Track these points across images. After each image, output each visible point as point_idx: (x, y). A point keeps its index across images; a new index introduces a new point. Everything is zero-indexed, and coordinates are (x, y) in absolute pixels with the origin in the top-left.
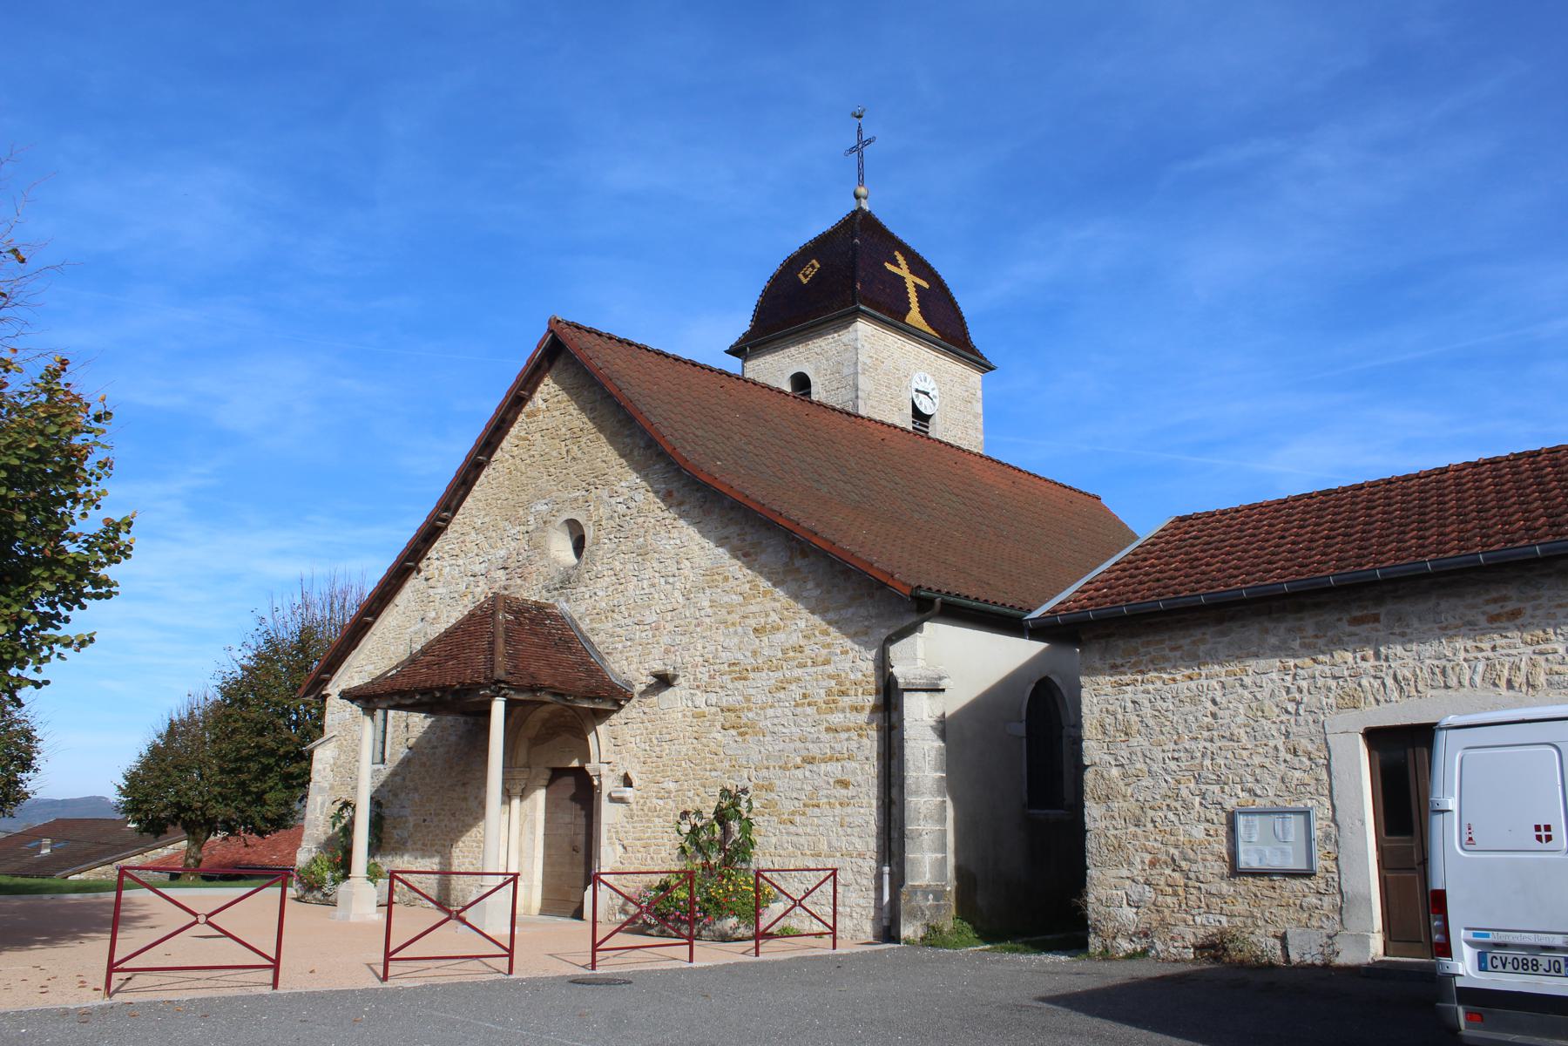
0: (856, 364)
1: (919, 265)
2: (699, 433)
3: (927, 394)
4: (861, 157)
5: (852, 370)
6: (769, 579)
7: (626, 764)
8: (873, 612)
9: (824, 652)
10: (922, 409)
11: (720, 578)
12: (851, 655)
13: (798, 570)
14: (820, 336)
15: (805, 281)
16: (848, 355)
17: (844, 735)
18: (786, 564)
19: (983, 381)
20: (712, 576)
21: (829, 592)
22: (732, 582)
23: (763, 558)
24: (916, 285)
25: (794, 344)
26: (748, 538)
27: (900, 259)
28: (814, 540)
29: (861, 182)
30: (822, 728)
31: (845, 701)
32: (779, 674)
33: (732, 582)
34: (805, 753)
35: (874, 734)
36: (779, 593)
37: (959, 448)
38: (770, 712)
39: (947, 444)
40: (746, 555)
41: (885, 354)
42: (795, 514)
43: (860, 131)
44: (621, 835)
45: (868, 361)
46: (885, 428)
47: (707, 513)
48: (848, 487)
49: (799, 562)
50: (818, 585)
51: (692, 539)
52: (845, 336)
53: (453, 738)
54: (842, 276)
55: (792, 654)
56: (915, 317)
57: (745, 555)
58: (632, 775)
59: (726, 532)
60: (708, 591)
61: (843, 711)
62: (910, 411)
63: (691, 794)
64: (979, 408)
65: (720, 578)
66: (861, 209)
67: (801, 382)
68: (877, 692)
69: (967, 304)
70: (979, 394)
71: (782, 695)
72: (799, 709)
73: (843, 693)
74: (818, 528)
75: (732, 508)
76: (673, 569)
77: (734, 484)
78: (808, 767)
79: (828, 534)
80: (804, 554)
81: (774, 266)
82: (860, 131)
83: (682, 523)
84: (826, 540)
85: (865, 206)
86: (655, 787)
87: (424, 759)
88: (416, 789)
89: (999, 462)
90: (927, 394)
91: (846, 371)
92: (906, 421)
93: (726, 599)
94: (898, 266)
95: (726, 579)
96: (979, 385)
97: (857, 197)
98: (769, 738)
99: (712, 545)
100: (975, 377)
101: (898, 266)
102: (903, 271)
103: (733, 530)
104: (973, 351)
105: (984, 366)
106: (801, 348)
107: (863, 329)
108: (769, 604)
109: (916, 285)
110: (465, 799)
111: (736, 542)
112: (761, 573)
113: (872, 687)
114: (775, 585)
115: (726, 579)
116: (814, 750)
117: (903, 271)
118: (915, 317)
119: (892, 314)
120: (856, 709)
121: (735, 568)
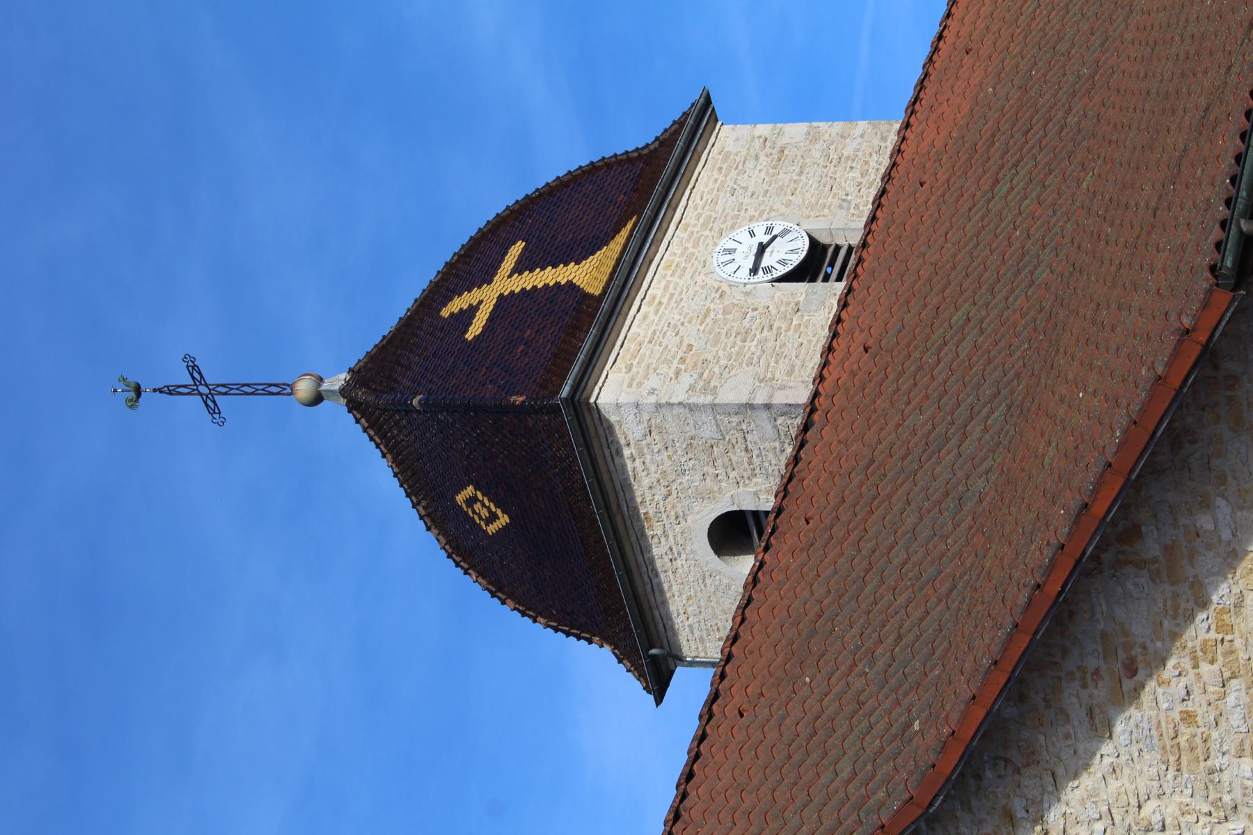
0: (691, 408)
1: (472, 264)
2: (845, 768)
3: (762, 248)
4: (229, 389)
5: (706, 418)
6: (1190, 618)
10: (796, 259)
11: (1186, 732)
13: (1169, 550)
14: (627, 487)
15: (504, 520)
16: (672, 426)
18: (1155, 577)
19: (734, 122)
20: (1181, 750)
21: (1222, 480)
22: (1197, 704)
23: (1140, 629)
24: (518, 269)
25: (644, 549)
26: (1091, 663)
27: (458, 304)
28: (1099, 509)
29: (285, 389)
33: (1198, 699)
36: (1222, 594)
37: (888, 177)
39: (878, 203)
40: (1132, 670)
41: (671, 341)
42: (1038, 553)
43: (171, 391)
45: (686, 379)
46: (840, 345)
47: (1031, 757)
48: (975, 429)
49: (1151, 547)
50: (1206, 504)
51: (1093, 794)
52: (628, 430)
54: (495, 439)
56: (588, 274)
57: (1132, 670)
59: (1077, 713)
60: (1216, 762)
62: (801, 287)
64: (795, 131)
65: (1186, 732)
66: (343, 392)
67: (731, 532)
69: (562, 153)
70: (763, 129)
74: (1074, 502)
75: (1022, 698)
77: (966, 691)
79: (1085, 479)
80: (1133, 534)
81: (468, 590)
82: (171, 391)
84: (1099, 483)
85: (337, 381)
89: (921, 86)
90: (762, 248)
91: (708, 431)
92: (823, 298)
93: (1236, 719)
94: (473, 310)
95: (1188, 717)
96: (743, 130)
97: (317, 399)
99: (1107, 748)
100: (727, 139)
101: (473, 310)
102: (485, 298)
103: (1073, 699)
104: (665, 142)
105: (699, 121)
106: (653, 530)
107: (614, 391)
109: (518, 269)
111: (1100, 692)
112: (1175, 636)
114: (1204, 604)
115: (1188, 717)
117: (485, 298)
118: (588, 274)
119: (585, 325)
121: (1161, 697)
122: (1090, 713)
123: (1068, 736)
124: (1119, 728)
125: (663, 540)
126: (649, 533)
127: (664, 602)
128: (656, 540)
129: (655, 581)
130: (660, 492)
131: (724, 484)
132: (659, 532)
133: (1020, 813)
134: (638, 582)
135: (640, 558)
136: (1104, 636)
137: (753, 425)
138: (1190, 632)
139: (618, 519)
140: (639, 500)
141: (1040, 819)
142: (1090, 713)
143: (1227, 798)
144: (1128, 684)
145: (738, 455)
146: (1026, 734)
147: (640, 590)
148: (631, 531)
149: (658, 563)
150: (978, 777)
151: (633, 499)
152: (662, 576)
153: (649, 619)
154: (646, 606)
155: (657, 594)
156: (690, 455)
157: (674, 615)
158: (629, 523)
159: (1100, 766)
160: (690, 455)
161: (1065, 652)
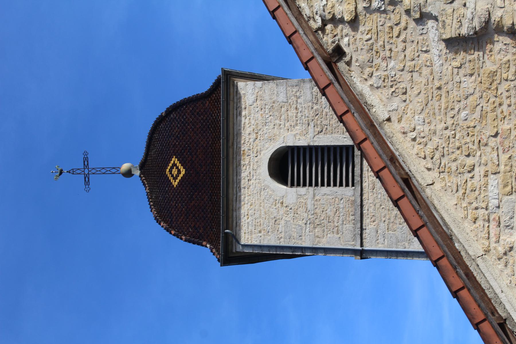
25: (238, 173)
106: (245, 161)
125: (248, 167)
126: (242, 163)
127: (240, 208)
128: (245, 167)
129: (238, 194)
130: (253, 136)
131: (282, 131)
132: (247, 163)
134: (230, 191)
135: (235, 178)
137: (302, 93)
139: (231, 150)
140: (242, 142)
145: (292, 112)
147: (231, 196)
148: (235, 161)
149: (243, 182)
151: (240, 142)
152: (242, 190)
153: (230, 215)
154: (231, 207)
155: (238, 202)
156: (271, 113)
157: (242, 216)
158: (235, 156)
160: (271, 113)
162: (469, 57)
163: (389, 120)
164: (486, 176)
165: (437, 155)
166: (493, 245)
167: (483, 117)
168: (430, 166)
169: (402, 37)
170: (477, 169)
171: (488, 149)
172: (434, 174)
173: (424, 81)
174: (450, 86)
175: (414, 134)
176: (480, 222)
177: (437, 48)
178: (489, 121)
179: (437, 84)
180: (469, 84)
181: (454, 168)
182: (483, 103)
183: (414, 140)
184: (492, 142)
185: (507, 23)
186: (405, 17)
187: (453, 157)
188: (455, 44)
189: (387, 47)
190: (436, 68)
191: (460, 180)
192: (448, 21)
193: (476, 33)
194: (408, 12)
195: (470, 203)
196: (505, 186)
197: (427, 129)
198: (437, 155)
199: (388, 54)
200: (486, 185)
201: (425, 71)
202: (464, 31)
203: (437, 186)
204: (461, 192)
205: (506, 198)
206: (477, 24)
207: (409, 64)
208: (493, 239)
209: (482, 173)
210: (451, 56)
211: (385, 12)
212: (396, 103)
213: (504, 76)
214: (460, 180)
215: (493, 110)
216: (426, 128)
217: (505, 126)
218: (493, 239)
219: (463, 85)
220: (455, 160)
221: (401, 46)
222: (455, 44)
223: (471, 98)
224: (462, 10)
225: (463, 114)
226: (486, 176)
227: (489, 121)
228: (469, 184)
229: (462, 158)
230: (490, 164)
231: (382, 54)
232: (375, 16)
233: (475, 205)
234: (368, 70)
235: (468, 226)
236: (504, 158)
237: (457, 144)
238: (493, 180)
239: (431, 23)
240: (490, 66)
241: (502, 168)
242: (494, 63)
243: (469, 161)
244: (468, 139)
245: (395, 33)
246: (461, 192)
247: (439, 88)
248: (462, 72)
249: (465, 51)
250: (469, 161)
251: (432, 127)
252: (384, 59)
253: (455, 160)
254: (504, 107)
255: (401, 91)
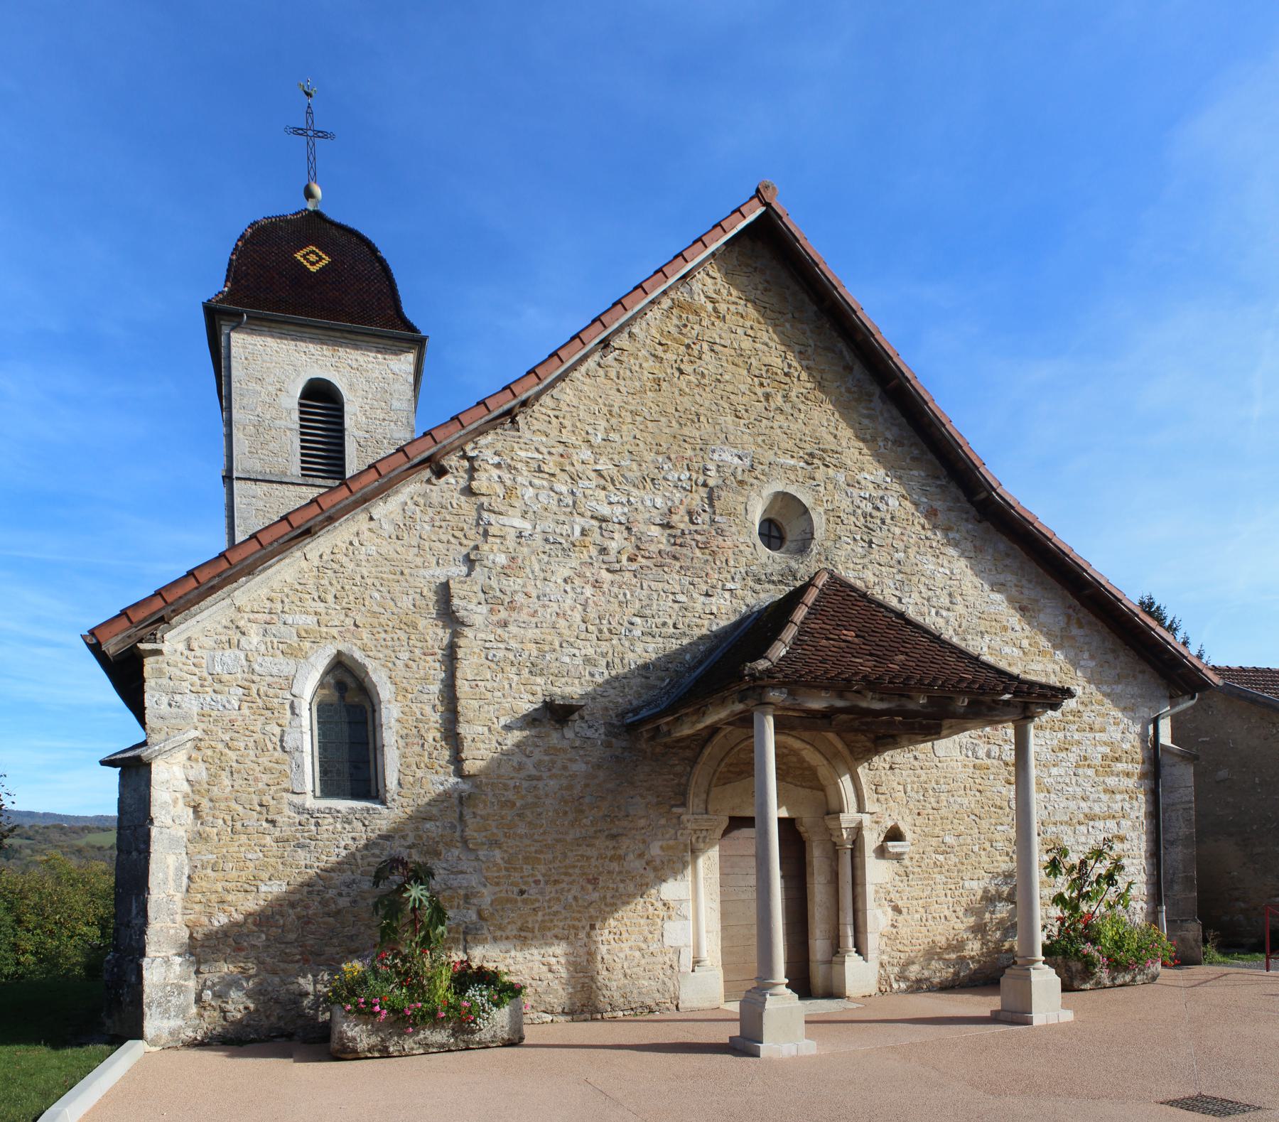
6: (1049, 641)
7: (895, 816)
8: (1136, 690)
9: (1099, 719)
12: (1122, 726)
13: (1073, 638)
17: (1118, 797)
30: (1100, 788)
31: (1120, 766)
32: (1061, 735)
34: (1087, 811)
35: (1142, 797)
36: (1060, 656)
38: (1054, 771)
40: (1023, 609)
44: (894, 896)
53: (579, 767)
55: (1071, 718)
58: (904, 828)
59: (1001, 578)
61: (1118, 775)
63: (976, 848)
68: (1143, 763)
71: (1063, 754)
72: (1080, 771)
73: (1118, 759)
76: (945, 601)
78: (1091, 823)
83: (951, 551)
86: (934, 842)
87: (510, 795)
88: (494, 843)
95: (1005, 629)
98: (1053, 796)
99: (986, 587)
103: (1010, 578)
108: (1050, 667)
110: (620, 858)
111: (1014, 591)
113: (1139, 757)
116: (1097, 809)
120: (1128, 775)
122: (1002, 585)
123: (990, 570)
124: (998, 597)
133: (951, 535)
136: (1037, 601)
138: (1043, 639)
141: (949, 544)
142: (1002, 585)
143: (969, 637)
144: (1017, 605)
146: (991, 551)
150: (967, 520)
159: (977, 581)
161: (1030, 582)
162: (431, 606)
163: (371, 519)
164: (316, 613)
165: (335, 566)
166: (246, 616)
167: (375, 614)
168: (325, 557)
169: (452, 540)
170: (322, 605)
171: (342, 617)
172: (316, 562)
173: (410, 559)
174: (404, 584)
175: (356, 543)
176: (268, 604)
177: (440, 574)
178: (370, 620)
179: (406, 571)
180: (406, 602)
181: (323, 582)
182: (388, 615)
183: (351, 543)
184: (349, 622)
185: (461, 642)
186: (472, 544)
187: (334, 582)
188: (444, 592)
189: (444, 524)
190: (422, 572)
191: (311, 586)
192: (465, 587)
193: (453, 612)
194: (476, 548)
195: (287, 596)
196: (306, 631)
197: (362, 557)
198: (335, 566)
199: (437, 524)
200: (307, 613)
201: (419, 561)
202: (455, 601)
203: (304, 564)
204: (299, 587)
205: (294, 632)
206: (461, 613)
207: (427, 544)
208: (252, 616)
209: (319, 610)
210: (433, 587)
211: (478, 524)
212: (388, 528)
213: (413, 637)
214: (311, 586)
215: (380, 624)
216: (362, 557)
217: (365, 635)
218: (252, 616)
219: (405, 597)
220: (331, 584)
221: (444, 538)
222: (444, 592)
223: (392, 603)
224: (475, 601)
225: (376, 595)
226: (316, 613)
227: (370, 620)
228: (308, 596)
229: (333, 591)
230: (328, 618)
231: (437, 518)
232: (474, 514)
233: (286, 600)
234: (421, 501)
235: (264, 592)
236: (334, 632)
237: (347, 587)
238: (311, 620)
239: (465, 569)
240: (422, 623)
241: (324, 629)
242: (425, 628)
243: (330, 598)
244: (352, 598)
245: (456, 533)
246: (299, 587)
247: (402, 573)
248: (418, 596)
249: (437, 601)
250: (330, 598)
251: (364, 563)
252: (432, 520)
253: (331, 584)
254: (383, 635)
255: (400, 534)
